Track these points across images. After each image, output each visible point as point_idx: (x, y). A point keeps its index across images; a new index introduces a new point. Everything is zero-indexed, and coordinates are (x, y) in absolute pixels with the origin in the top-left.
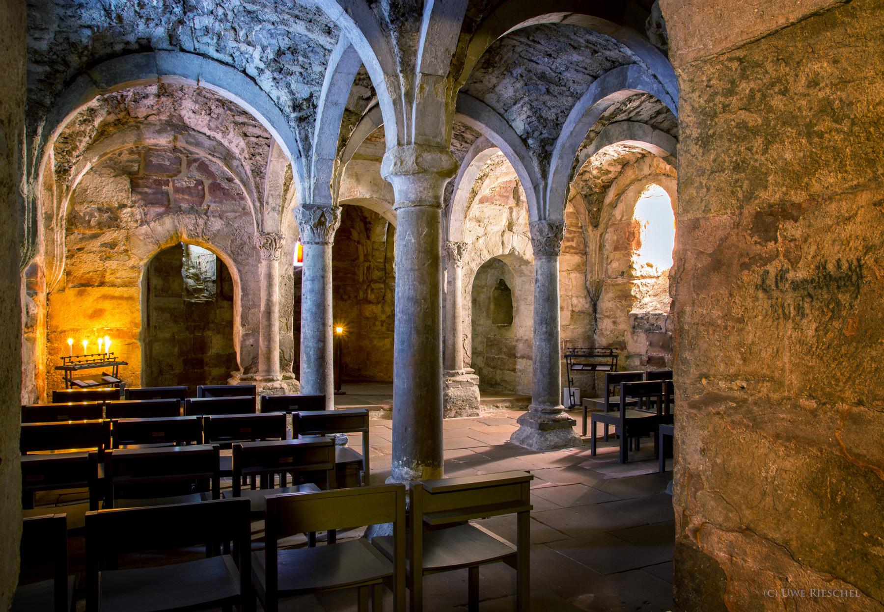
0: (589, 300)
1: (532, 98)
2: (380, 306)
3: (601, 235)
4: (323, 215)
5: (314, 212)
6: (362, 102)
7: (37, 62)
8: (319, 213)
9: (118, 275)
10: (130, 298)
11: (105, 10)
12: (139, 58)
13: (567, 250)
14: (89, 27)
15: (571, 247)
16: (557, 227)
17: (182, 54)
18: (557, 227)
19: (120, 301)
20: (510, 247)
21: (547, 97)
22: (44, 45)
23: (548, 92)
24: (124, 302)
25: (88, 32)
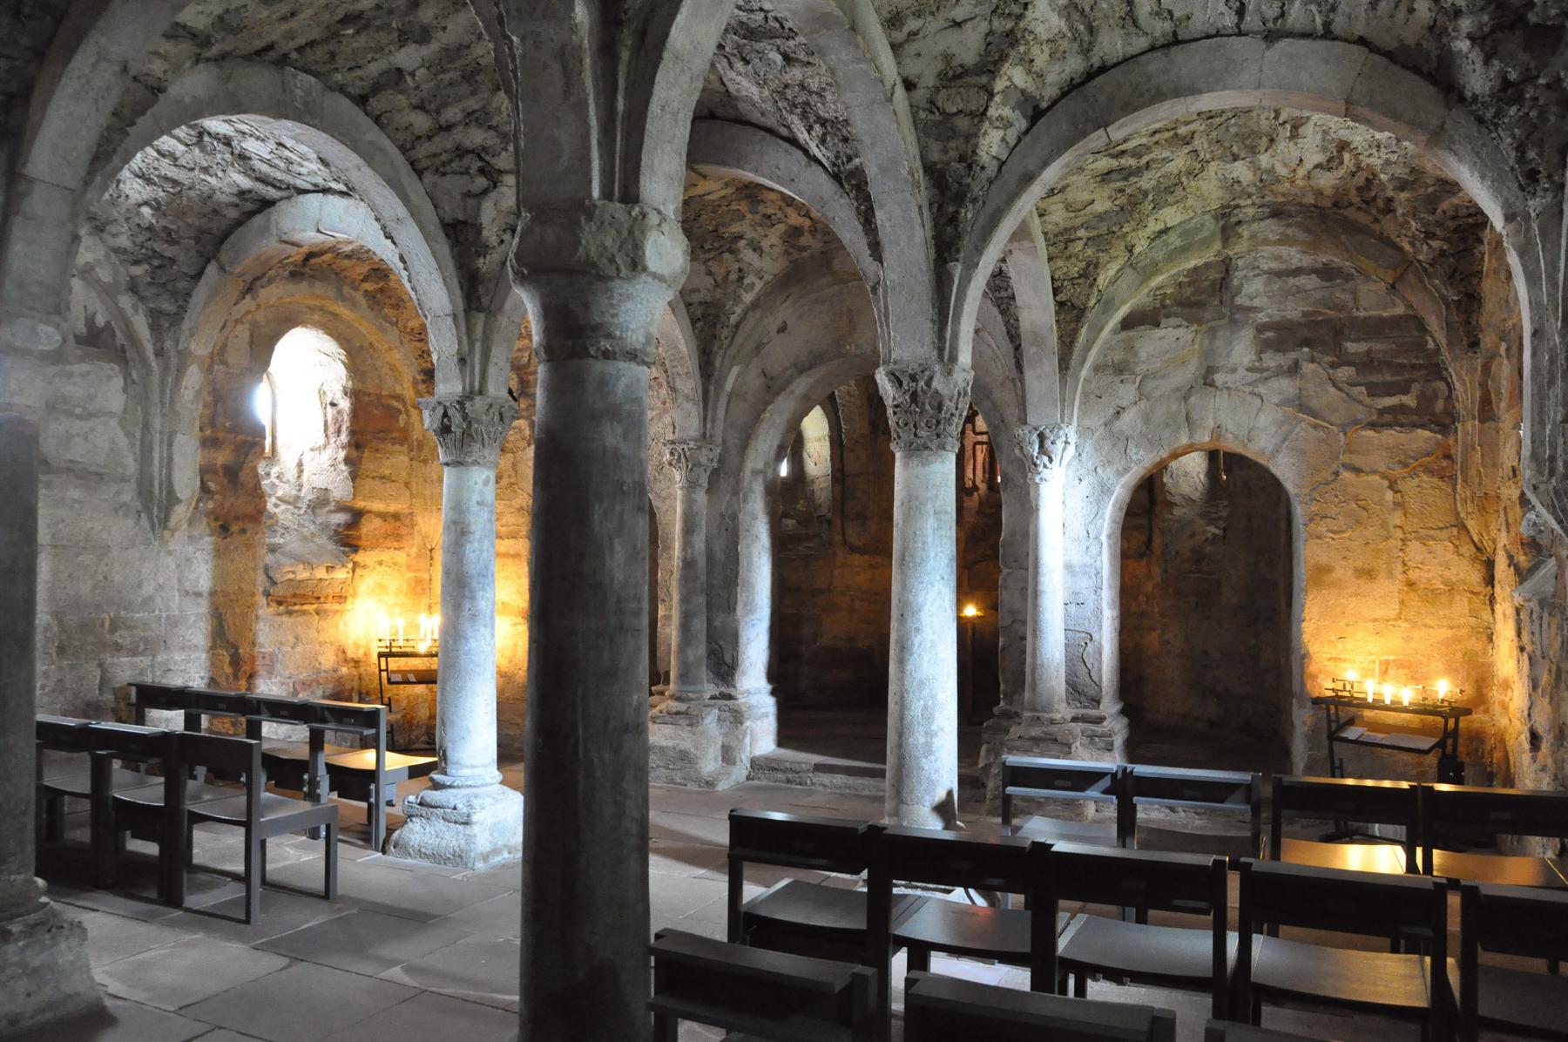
0: (1467, 549)
1: (773, 86)
2: (1144, 562)
3: (1486, 368)
4: (445, 415)
5: (434, 409)
6: (471, 202)
7: (137, 262)
8: (440, 411)
9: (504, 521)
10: (517, 556)
11: (137, 176)
12: (258, 220)
13: (1388, 418)
14: (146, 203)
15: (1402, 408)
16: (913, 378)
17: (301, 197)
18: (913, 378)
19: (506, 560)
20: (1211, 424)
21: (796, 73)
22: (124, 241)
23: (788, 59)
24: (509, 561)
25: (146, 210)
